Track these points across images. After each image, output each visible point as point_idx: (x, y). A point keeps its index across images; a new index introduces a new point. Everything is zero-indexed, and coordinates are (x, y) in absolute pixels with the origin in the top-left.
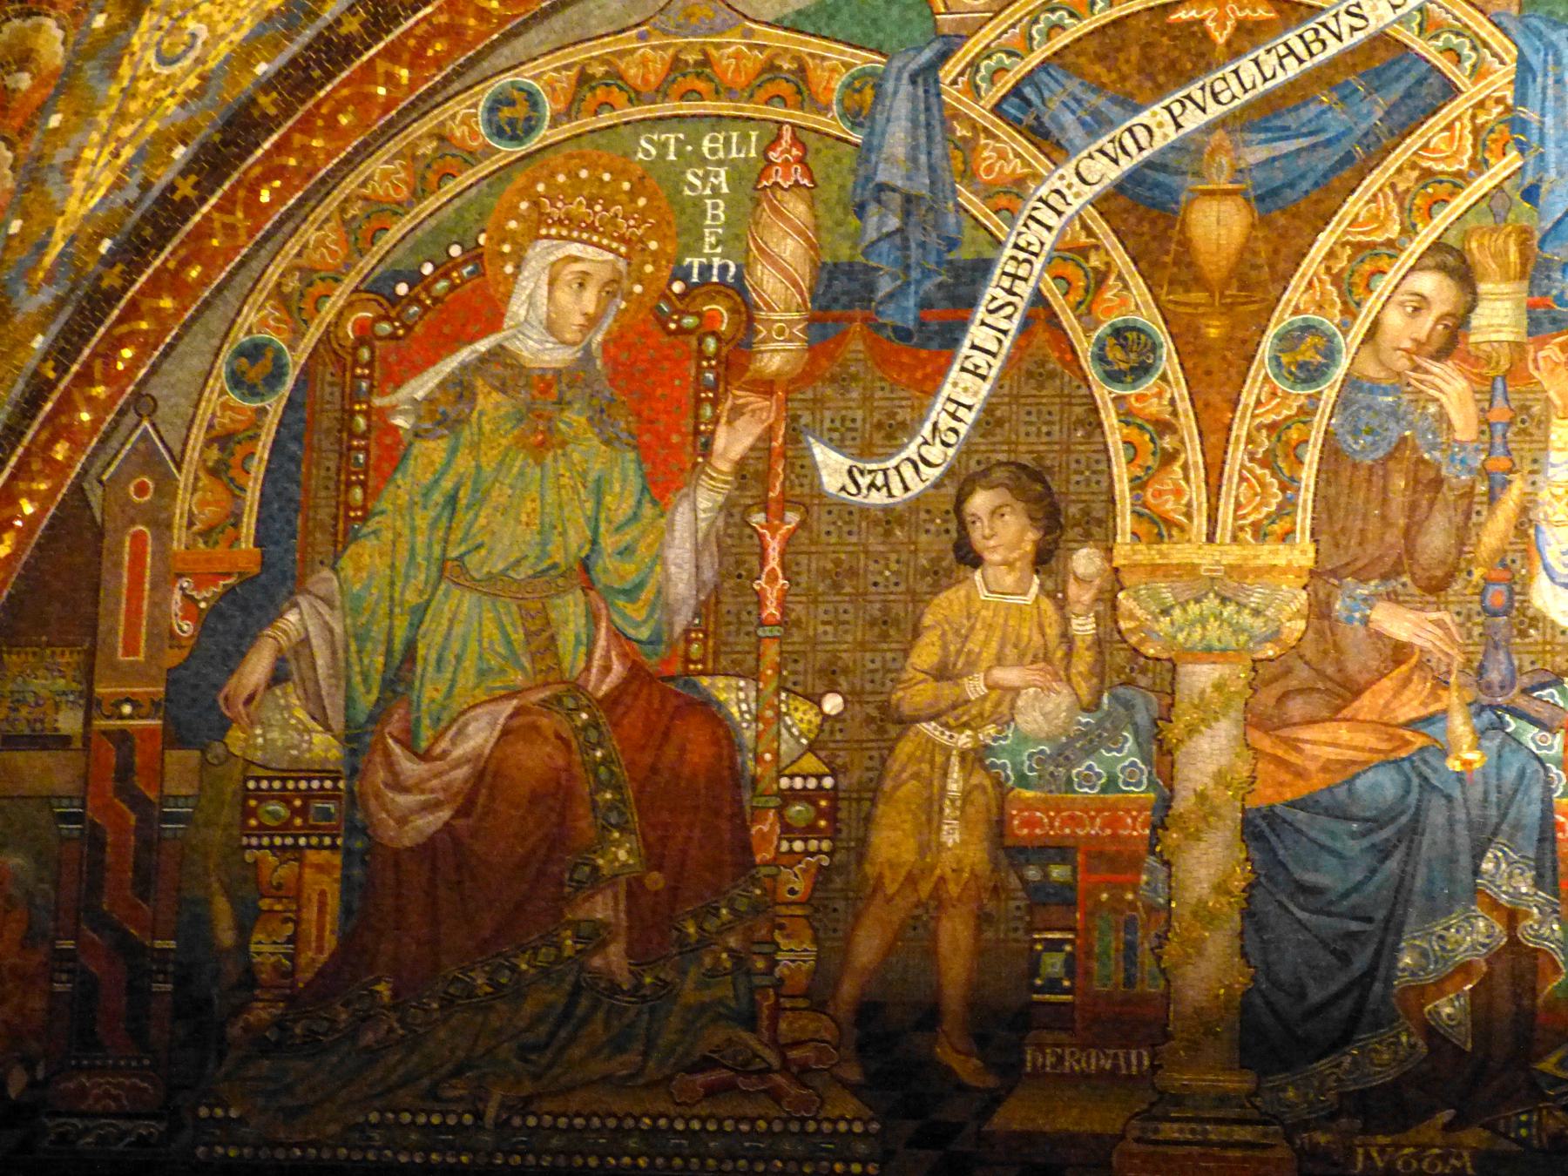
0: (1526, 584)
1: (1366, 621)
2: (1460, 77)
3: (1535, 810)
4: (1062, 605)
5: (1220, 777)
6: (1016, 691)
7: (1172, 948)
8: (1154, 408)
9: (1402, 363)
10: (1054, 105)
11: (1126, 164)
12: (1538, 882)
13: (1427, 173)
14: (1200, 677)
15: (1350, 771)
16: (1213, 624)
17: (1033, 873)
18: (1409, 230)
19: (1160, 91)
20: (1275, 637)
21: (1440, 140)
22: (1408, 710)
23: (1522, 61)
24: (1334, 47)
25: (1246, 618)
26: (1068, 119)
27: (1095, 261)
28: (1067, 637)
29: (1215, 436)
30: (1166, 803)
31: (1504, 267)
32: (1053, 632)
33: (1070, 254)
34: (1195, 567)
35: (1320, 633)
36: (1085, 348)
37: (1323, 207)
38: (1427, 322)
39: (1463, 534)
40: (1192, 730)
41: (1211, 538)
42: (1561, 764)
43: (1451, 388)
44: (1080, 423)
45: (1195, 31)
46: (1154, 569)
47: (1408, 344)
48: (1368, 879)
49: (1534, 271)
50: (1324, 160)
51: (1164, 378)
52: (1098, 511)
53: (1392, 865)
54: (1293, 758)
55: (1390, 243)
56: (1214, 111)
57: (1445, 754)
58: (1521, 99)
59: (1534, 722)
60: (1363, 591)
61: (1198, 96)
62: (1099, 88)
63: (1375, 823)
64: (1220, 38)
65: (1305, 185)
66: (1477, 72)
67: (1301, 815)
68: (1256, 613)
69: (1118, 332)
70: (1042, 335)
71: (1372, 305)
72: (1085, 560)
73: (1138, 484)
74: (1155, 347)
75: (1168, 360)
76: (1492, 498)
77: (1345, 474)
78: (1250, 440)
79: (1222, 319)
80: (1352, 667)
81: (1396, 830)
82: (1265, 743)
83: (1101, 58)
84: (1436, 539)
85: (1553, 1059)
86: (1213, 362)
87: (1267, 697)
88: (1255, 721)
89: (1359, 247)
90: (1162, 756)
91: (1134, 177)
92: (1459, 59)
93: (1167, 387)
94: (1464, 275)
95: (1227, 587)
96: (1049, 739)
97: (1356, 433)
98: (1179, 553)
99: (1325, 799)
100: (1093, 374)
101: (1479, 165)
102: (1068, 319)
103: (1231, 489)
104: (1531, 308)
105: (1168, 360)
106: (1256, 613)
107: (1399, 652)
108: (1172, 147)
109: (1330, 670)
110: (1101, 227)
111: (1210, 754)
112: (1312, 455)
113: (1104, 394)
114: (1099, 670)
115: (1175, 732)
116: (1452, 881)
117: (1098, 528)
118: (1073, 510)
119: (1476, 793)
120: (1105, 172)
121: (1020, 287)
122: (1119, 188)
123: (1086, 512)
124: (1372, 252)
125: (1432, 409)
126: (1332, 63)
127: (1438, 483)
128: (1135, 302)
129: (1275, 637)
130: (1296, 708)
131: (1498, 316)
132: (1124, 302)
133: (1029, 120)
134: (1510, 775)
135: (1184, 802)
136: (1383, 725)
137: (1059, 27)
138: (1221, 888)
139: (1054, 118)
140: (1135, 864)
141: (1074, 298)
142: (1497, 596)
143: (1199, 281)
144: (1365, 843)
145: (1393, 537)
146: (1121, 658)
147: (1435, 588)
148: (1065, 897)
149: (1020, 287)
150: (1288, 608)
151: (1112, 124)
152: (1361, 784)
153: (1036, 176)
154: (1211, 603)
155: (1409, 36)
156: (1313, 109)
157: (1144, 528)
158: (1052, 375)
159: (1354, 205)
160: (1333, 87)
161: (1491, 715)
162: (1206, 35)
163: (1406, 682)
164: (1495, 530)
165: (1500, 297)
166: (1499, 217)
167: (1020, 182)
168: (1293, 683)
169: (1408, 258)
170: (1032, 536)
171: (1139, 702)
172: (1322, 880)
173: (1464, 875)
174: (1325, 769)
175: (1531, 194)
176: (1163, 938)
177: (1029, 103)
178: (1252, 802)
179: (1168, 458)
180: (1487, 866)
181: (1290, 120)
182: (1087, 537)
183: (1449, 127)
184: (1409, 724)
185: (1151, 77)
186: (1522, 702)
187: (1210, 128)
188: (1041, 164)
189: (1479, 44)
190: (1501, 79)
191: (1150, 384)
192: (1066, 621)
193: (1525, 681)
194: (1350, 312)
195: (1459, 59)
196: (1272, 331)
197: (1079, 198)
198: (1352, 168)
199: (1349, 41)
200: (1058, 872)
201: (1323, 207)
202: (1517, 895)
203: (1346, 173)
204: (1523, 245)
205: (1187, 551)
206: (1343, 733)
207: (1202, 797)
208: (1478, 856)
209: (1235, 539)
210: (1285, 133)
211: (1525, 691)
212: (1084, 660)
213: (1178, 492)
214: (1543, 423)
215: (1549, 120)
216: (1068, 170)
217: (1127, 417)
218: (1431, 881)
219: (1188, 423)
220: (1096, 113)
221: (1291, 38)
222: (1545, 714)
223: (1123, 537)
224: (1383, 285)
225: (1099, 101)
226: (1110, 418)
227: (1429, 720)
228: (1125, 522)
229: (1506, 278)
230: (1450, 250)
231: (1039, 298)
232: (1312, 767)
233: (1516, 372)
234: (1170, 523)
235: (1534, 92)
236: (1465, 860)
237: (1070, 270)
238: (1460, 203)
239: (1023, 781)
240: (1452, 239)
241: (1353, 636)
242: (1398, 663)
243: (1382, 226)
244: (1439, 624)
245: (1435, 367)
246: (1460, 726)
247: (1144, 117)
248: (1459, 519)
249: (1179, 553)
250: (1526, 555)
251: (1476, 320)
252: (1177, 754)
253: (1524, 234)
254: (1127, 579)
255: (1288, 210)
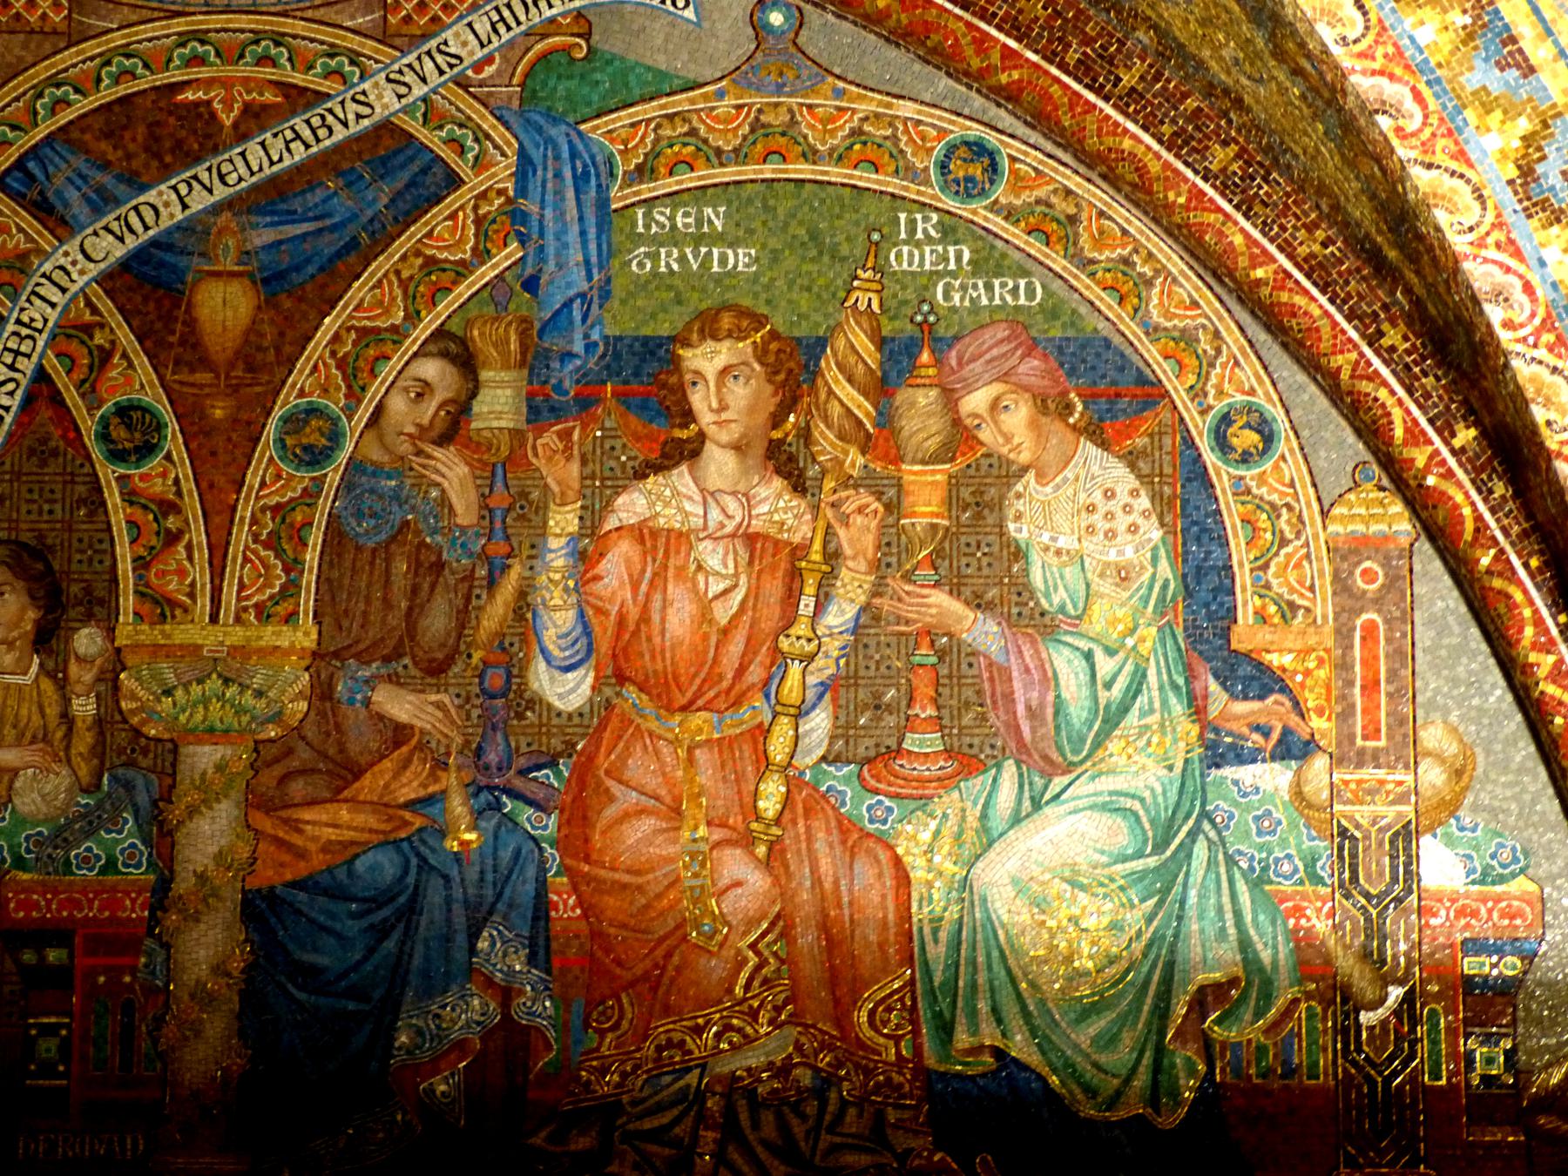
0: (525, 665)
1: (367, 702)
2: (463, 168)
3: (530, 888)
4: (62, 685)
5: (219, 856)
6: (15, 772)
7: (170, 1030)
8: (158, 487)
9: (405, 448)
10: (59, 181)
11: (131, 243)
12: (532, 960)
13: (431, 262)
14: (203, 757)
15: (350, 852)
16: (215, 706)
17: (28, 957)
18: (413, 317)
19: (166, 172)
20: (277, 718)
21: (443, 228)
22: (408, 791)
23: (522, 153)
24: (340, 134)
25: (248, 699)
26: (73, 195)
27: (99, 339)
28: (67, 718)
29: (219, 517)
30: (164, 885)
31: (504, 354)
32: (52, 712)
33: (73, 332)
34: (199, 647)
35: (322, 714)
36: (88, 426)
37: (330, 292)
38: (429, 408)
39: (464, 616)
40: (193, 811)
41: (214, 619)
42: (555, 844)
43: (452, 473)
44: (82, 502)
45: (201, 113)
46: (156, 650)
47: (410, 429)
48: (365, 959)
49: (534, 360)
50: (328, 245)
51: (168, 457)
52: (100, 592)
53: (390, 945)
54: (297, 840)
55: (394, 329)
56: (221, 193)
57: (443, 834)
58: (522, 191)
59: (530, 803)
60: (365, 673)
61: (205, 176)
62: (106, 166)
63: (376, 901)
64: (227, 120)
65: (311, 269)
66: (480, 164)
67: (302, 896)
68: (259, 694)
69: (123, 411)
70: (45, 413)
71: (375, 390)
72: (86, 640)
73: (141, 565)
74: (160, 427)
75: (173, 439)
76: (492, 583)
77: (349, 557)
78: (254, 521)
79: (227, 396)
80: (353, 748)
81: (396, 909)
82: (265, 823)
83: (108, 135)
84: (437, 621)
85: (543, 1134)
86: (219, 442)
87: (269, 778)
88: (256, 802)
89: (363, 332)
90: (162, 838)
91: (139, 255)
92: (462, 151)
93: (172, 466)
94: (466, 362)
95: (230, 668)
96: (45, 821)
97: (359, 515)
98: (183, 633)
99: (325, 880)
100: (97, 453)
101: (482, 255)
102: (72, 397)
103: (234, 571)
104: (531, 396)
105: (173, 439)
106: (259, 694)
107: (400, 734)
108: (178, 227)
109: (332, 752)
110: (106, 305)
111: (211, 835)
112: (316, 538)
113: (108, 473)
114: (99, 750)
115: (176, 813)
116: (448, 959)
117: (100, 607)
118: (75, 589)
119: (472, 874)
120: (110, 250)
121: (22, 363)
122: (125, 265)
123: (88, 591)
124: (374, 341)
125: (434, 494)
126: (338, 148)
127: (439, 566)
128: (140, 380)
129: (277, 718)
130: (298, 788)
131: (498, 403)
132: (129, 381)
133: (33, 194)
134: (506, 855)
135: (183, 884)
136: (383, 806)
137: (61, 103)
138: (219, 970)
139: (59, 193)
140: (132, 946)
141: (78, 375)
142: (495, 679)
143: (205, 362)
144: (364, 923)
145: (395, 620)
146: (122, 738)
147: (436, 670)
148: (61, 977)
149: (22, 363)
150: (292, 693)
151: (118, 203)
152: (360, 865)
153: (39, 251)
154: (214, 684)
155: (414, 126)
156: (319, 194)
157: (147, 608)
158: (55, 453)
159: (359, 290)
160: (339, 173)
161: (488, 796)
162: (213, 115)
163: (406, 764)
164: (495, 612)
165: (501, 384)
166: (501, 307)
167: (23, 256)
168: (296, 764)
169: (412, 345)
170: (32, 614)
171: (140, 782)
172: (323, 960)
173: (460, 955)
174: (324, 850)
175: (531, 284)
176: (159, 1021)
177: (31, 178)
178: (253, 883)
179: (172, 538)
180: (483, 945)
181: (297, 204)
182: (88, 618)
183: (453, 216)
184: (409, 805)
185: (158, 156)
186: (518, 783)
187: (216, 209)
188: (46, 241)
189: (481, 136)
190: (502, 172)
191: (155, 463)
192: (66, 701)
193: (522, 762)
194: (354, 397)
195: (462, 151)
196: (277, 413)
197: (83, 276)
198: (356, 253)
199: (354, 129)
200: (53, 955)
201: (330, 292)
202: (511, 972)
203: (352, 258)
204: (523, 335)
205: (191, 632)
206: (344, 814)
207: (202, 878)
208: (474, 936)
209: (238, 619)
210: (291, 217)
211: (523, 773)
212: (84, 741)
213: (182, 573)
214: (542, 509)
215: (548, 213)
216: (72, 246)
217: (130, 496)
218: (427, 959)
219: (192, 504)
220: (100, 190)
221: (298, 122)
222: (541, 794)
223: (126, 617)
224: (388, 371)
225: (106, 179)
226: (113, 498)
227: (429, 800)
228: (128, 601)
229: (506, 366)
230: (451, 336)
231: (41, 375)
232: (312, 847)
233: (516, 459)
234: (173, 604)
235: (534, 186)
236: (461, 939)
237: (74, 347)
238: (464, 291)
239: (20, 863)
240: (455, 327)
241: (354, 717)
242: (398, 744)
243: (387, 312)
244: (439, 706)
245: (438, 453)
246: (458, 806)
247: (151, 196)
248: (460, 602)
249: (183, 633)
250: (525, 641)
251: (478, 407)
252: (179, 836)
253: (525, 322)
254: (130, 660)
255: (295, 291)
